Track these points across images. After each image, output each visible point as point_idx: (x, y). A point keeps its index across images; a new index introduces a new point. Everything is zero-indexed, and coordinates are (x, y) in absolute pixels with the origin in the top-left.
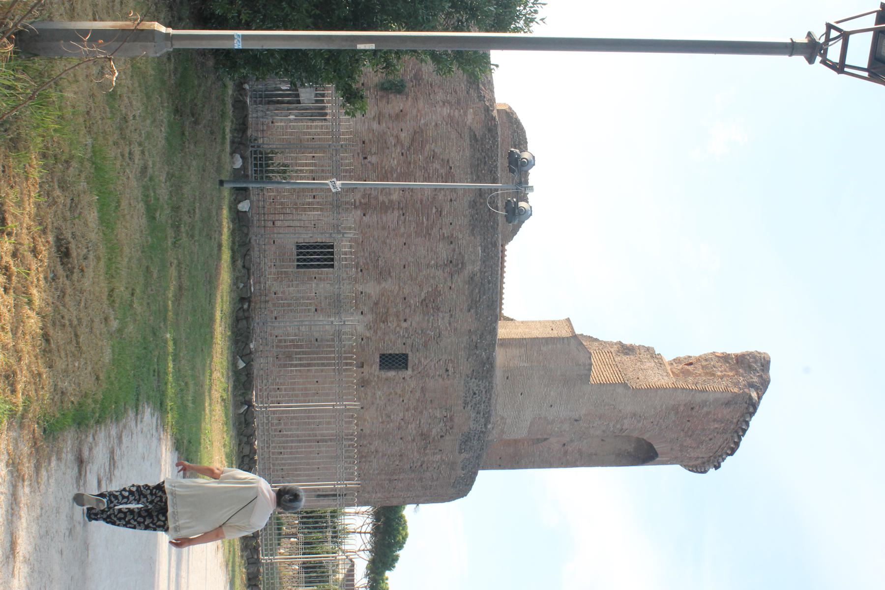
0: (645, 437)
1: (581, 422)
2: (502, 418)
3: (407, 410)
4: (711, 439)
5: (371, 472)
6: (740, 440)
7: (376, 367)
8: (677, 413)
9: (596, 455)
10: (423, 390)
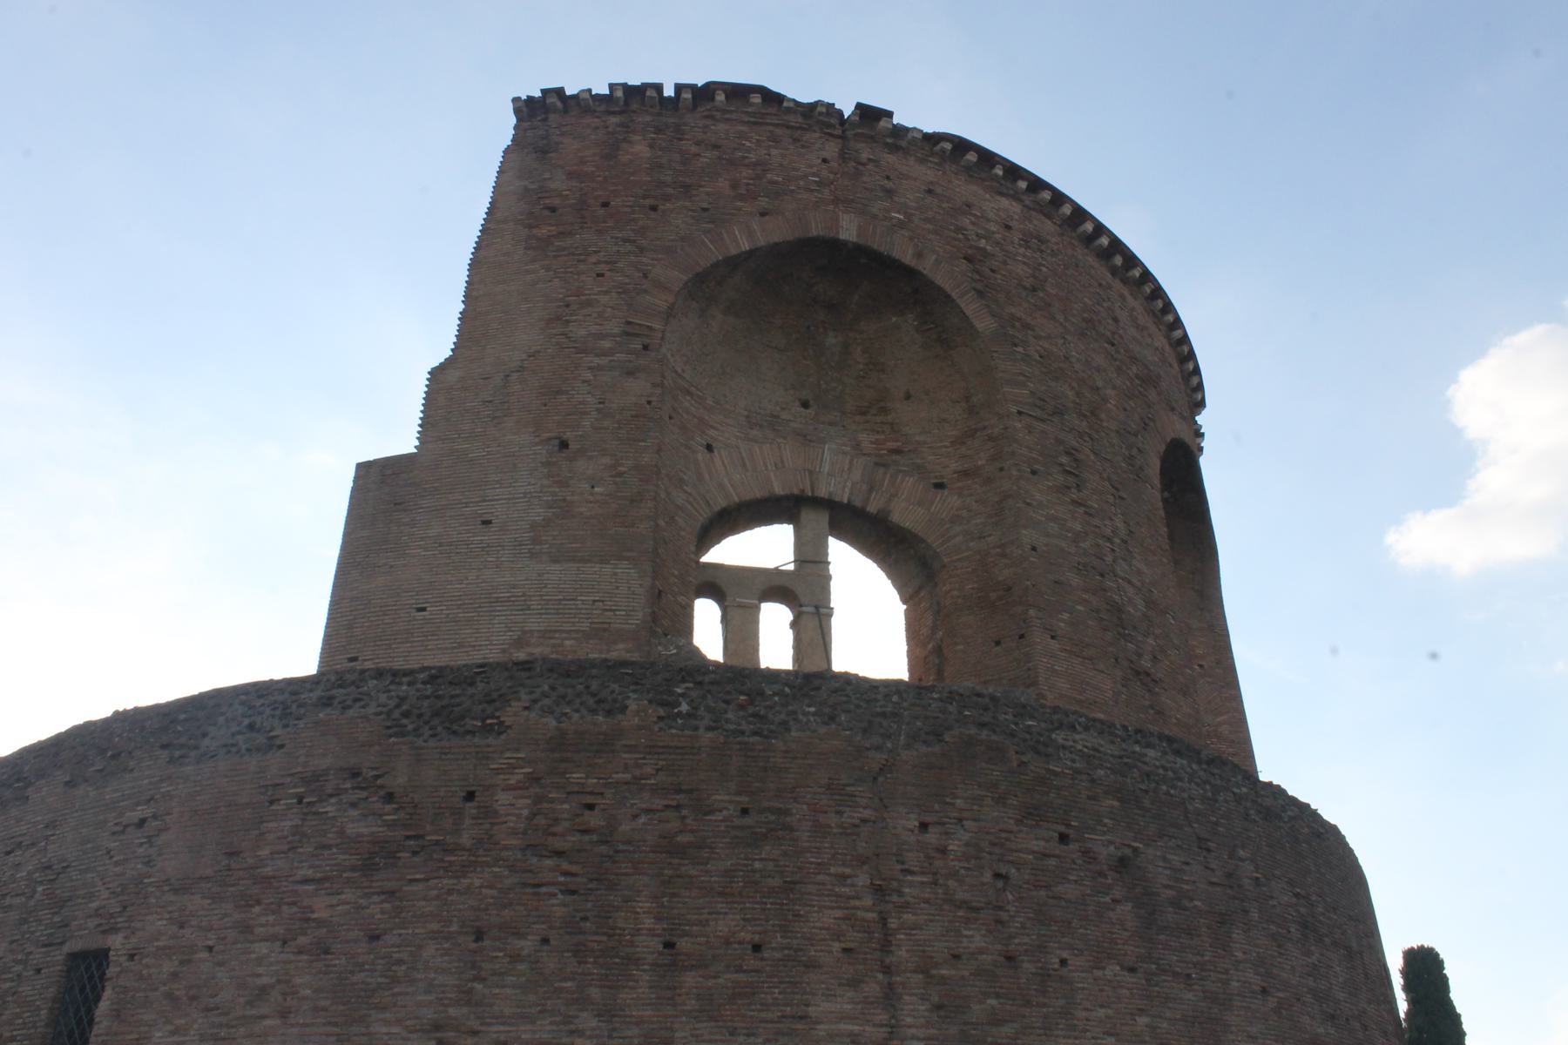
1: (568, 435)
2: (520, 643)
3: (246, 929)
4: (716, 147)
6: (679, 88)
9: (967, 399)
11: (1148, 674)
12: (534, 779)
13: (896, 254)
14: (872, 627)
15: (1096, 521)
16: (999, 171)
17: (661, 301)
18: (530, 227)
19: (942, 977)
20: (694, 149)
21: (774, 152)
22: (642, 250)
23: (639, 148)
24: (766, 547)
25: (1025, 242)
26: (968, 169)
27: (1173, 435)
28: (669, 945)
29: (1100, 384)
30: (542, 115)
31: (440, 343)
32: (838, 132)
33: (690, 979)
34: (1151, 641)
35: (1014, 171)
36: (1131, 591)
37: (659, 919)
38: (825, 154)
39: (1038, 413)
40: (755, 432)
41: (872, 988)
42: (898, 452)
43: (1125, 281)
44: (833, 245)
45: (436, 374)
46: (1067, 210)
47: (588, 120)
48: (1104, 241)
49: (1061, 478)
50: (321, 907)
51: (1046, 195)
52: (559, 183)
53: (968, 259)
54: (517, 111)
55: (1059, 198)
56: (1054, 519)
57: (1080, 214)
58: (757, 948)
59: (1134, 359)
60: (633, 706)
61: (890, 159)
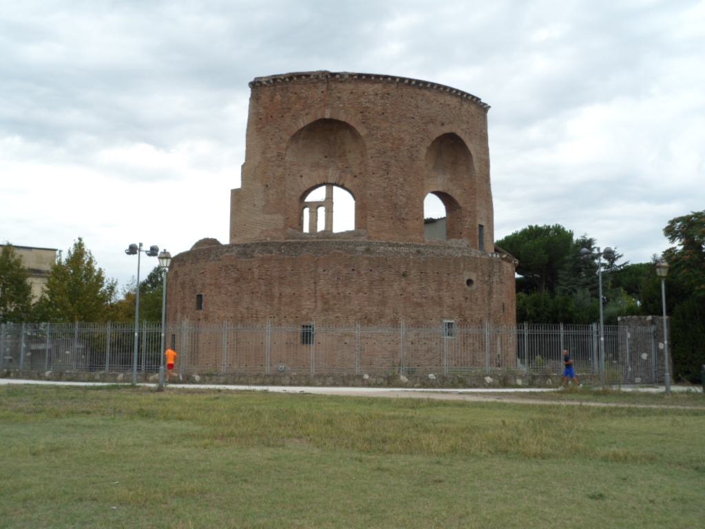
0: (288, 138)
2: (262, 232)
4: (296, 93)
5: (268, 310)
7: (201, 312)
8: (263, 127)
10: (211, 285)
11: (404, 219)
12: (259, 266)
13: (340, 119)
14: (343, 212)
15: (393, 182)
16: (373, 78)
17: (284, 145)
18: (257, 125)
19: (326, 298)
20: (291, 95)
21: (310, 93)
22: (280, 130)
23: (278, 97)
24: (318, 195)
25: (382, 98)
26: (364, 80)
27: (437, 135)
28: (280, 294)
29: (402, 136)
30: (256, 85)
31: (243, 161)
32: (326, 81)
33: (284, 299)
34: (407, 209)
35: (377, 77)
36: (401, 197)
37: (279, 290)
38: (323, 90)
39: (378, 155)
40: (313, 169)
41: (313, 300)
42: (347, 167)
43: (426, 88)
44: (325, 120)
45: (243, 166)
46: (398, 80)
47: (267, 89)
48: (413, 83)
49: (383, 172)
50: (230, 289)
51: (390, 79)
52: (261, 110)
53: (361, 113)
54: (251, 87)
55: (394, 78)
56: (377, 186)
57: (402, 80)
58: (294, 294)
59: (422, 118)
60: (274, 251)
61: (340, 86)
